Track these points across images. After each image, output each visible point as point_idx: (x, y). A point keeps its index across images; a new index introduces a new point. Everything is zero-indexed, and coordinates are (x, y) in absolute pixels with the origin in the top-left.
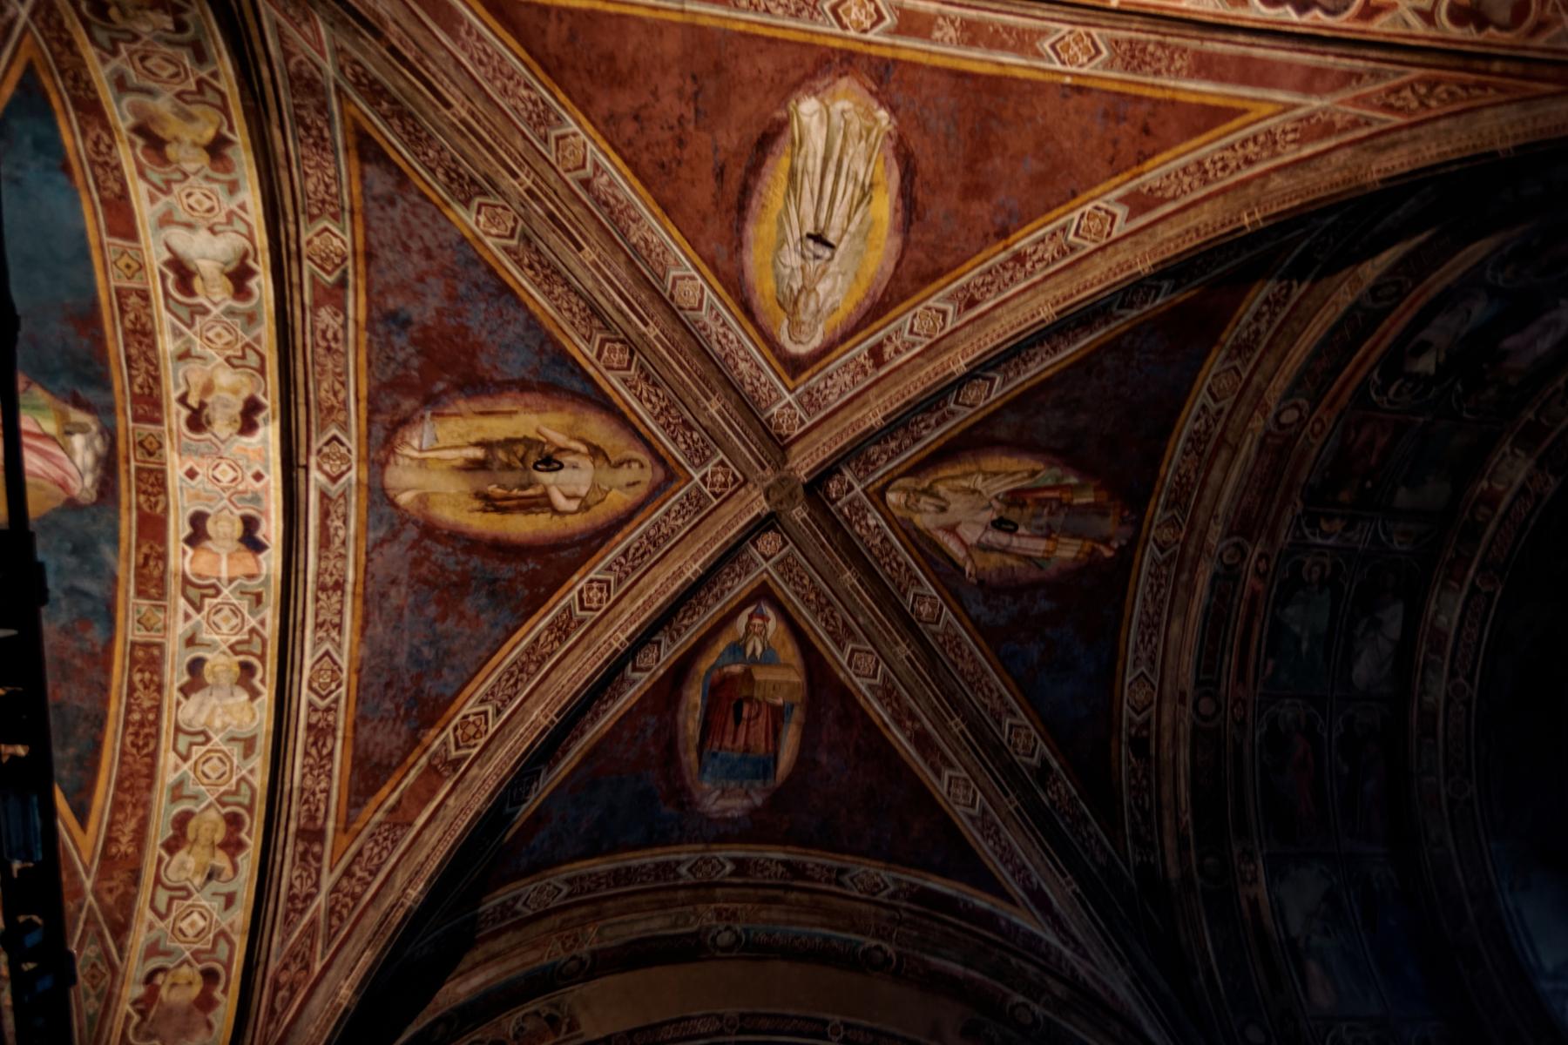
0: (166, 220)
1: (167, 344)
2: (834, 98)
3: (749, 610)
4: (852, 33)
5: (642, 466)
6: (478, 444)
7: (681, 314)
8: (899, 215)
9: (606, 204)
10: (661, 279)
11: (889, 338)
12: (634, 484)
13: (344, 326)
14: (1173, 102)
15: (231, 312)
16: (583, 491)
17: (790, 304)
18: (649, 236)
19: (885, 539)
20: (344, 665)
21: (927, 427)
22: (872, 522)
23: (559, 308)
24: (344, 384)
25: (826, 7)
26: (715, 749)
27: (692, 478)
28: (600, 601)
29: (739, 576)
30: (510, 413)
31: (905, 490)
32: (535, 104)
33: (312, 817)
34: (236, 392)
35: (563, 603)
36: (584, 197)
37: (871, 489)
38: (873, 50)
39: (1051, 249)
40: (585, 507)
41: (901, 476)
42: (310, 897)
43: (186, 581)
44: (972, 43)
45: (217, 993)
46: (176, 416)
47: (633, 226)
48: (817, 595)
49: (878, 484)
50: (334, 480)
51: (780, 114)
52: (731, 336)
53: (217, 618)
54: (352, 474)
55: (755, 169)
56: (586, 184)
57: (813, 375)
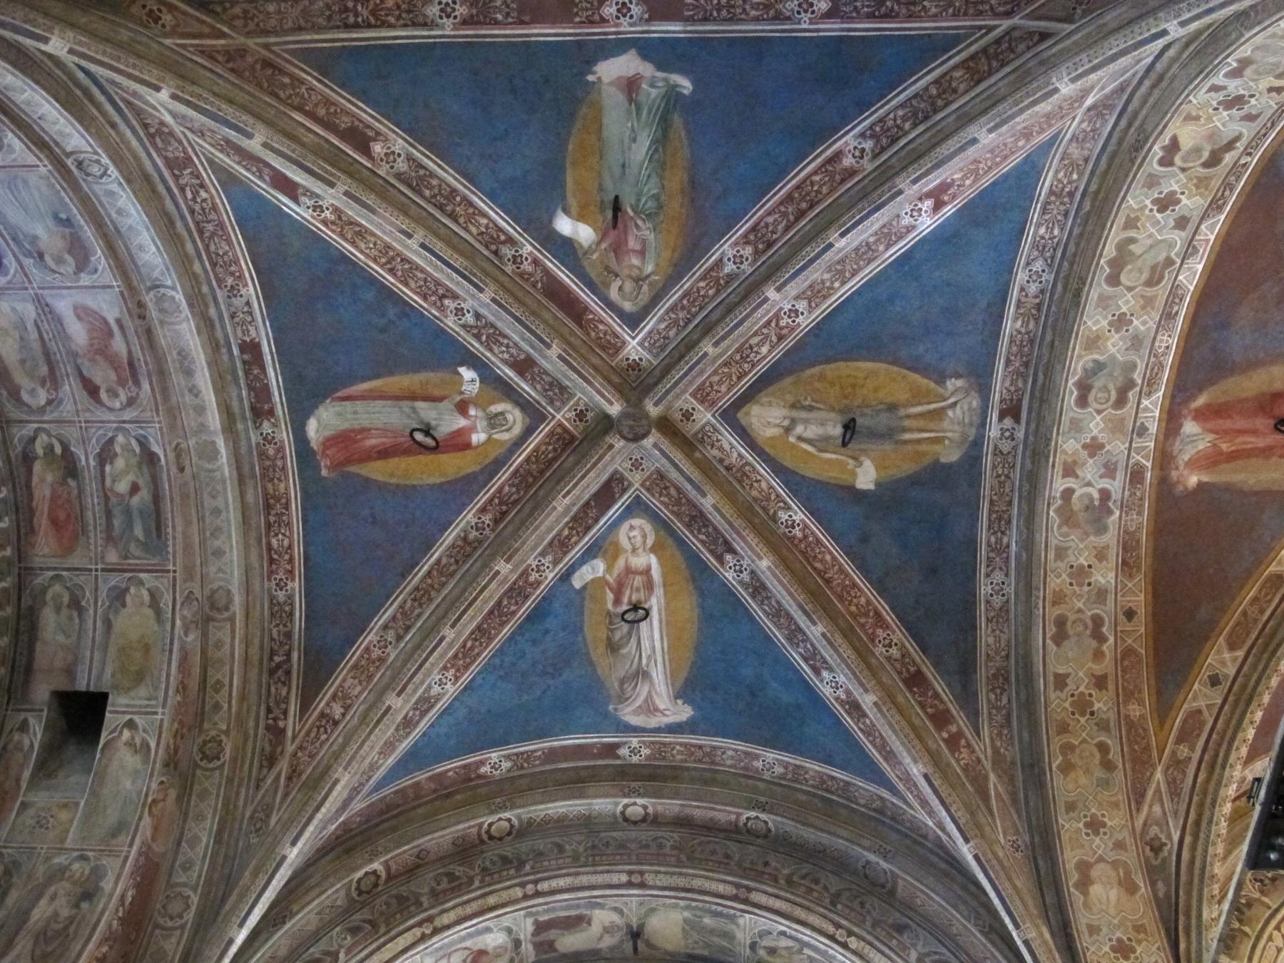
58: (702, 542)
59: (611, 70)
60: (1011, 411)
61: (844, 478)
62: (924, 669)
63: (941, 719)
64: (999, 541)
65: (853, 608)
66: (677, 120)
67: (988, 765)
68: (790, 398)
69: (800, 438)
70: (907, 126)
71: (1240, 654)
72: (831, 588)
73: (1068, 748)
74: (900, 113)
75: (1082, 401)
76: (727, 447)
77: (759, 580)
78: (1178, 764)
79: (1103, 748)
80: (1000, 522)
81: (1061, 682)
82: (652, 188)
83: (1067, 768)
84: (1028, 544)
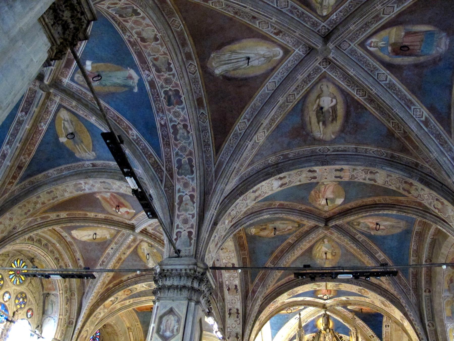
0: (272, 190)
1: (298, 183)
2: (212, 67)
3: (368, 48)
4: (197, 68)
5: (322, 85)
6: (318, 123)
7: (277, 86)
8: (236, 42)
9: (252, 113)
10: (268, 94)
11: (272, 32)
12: (327, 86)
13: (292, 153)
14: (175, 4)
15: (289, 177)
16: (330, 99)
17: (269, 59)
18: (258, 100)
19: (340, 12)
20: (376, 149)
21: (298, 12)
22: (335, 17)
23: (280, 115)
24: (306, 150)
25: (193, 76)
26: (420, 51)
27: (325, 71)
28: (363, 91)
29: (356, 53)
30: (310, 118)
31: (322, 10)
32: (233, 138)
33: (413, 163)
34: (307, 174)
35: (363, 101)
36: (251, 120)
37: (323, 20)
38: (199, 63)
39: (229, 9)
40: (335, 97)
41: (316, 13)
42: (431, 170)
43: (351, 179)
44: (187, 44)
45: (442, 201)
46: (313, 181)
47: (257, 105)
48: (363, 28)
49: (321, 19)
50: (329, 150)
51: (221, 78)
52: (281, 71)
53: (359, 175)
54: (327, 147)
55: (236, 79)
56: (248, 120)
57: (289, 46)
58: (24, 105)
59: (132, 72)
60: (94, 165)
61: (59, 134)
62: (24, 168)
63: (14, 177)
64: (64, 170)
65: (29, 147)
66: (127, 89)
67: (10, 191)
68: (72, 119)
69: (64, 123)
70: (141, 147)
71: (67, 217)
72: (31, 140)
73: (25, 206)
74: (143, 145)
75: (101, 182)
76: (53, 106)
77: (23, 122)
78: (36, 220)
79: (29, 211)
80: (69, 169)
81: (39, 197)
82: (108, 83)
83: (20, 208)
84: (66, 177)
